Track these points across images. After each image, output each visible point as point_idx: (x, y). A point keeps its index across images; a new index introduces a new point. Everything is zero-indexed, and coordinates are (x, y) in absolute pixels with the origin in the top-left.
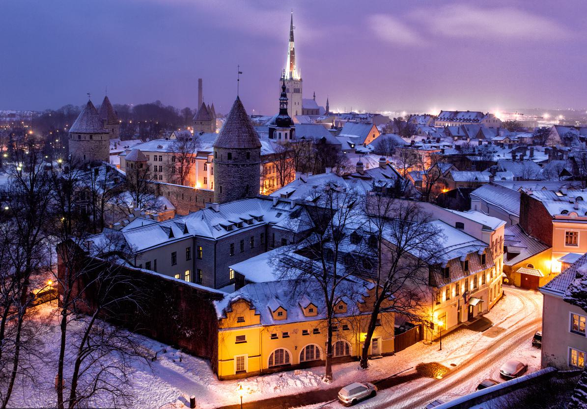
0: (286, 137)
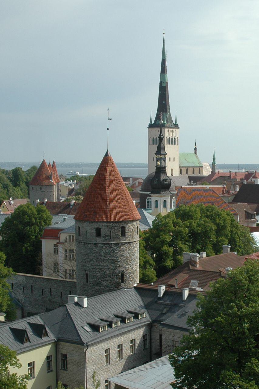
0: (165, 206)
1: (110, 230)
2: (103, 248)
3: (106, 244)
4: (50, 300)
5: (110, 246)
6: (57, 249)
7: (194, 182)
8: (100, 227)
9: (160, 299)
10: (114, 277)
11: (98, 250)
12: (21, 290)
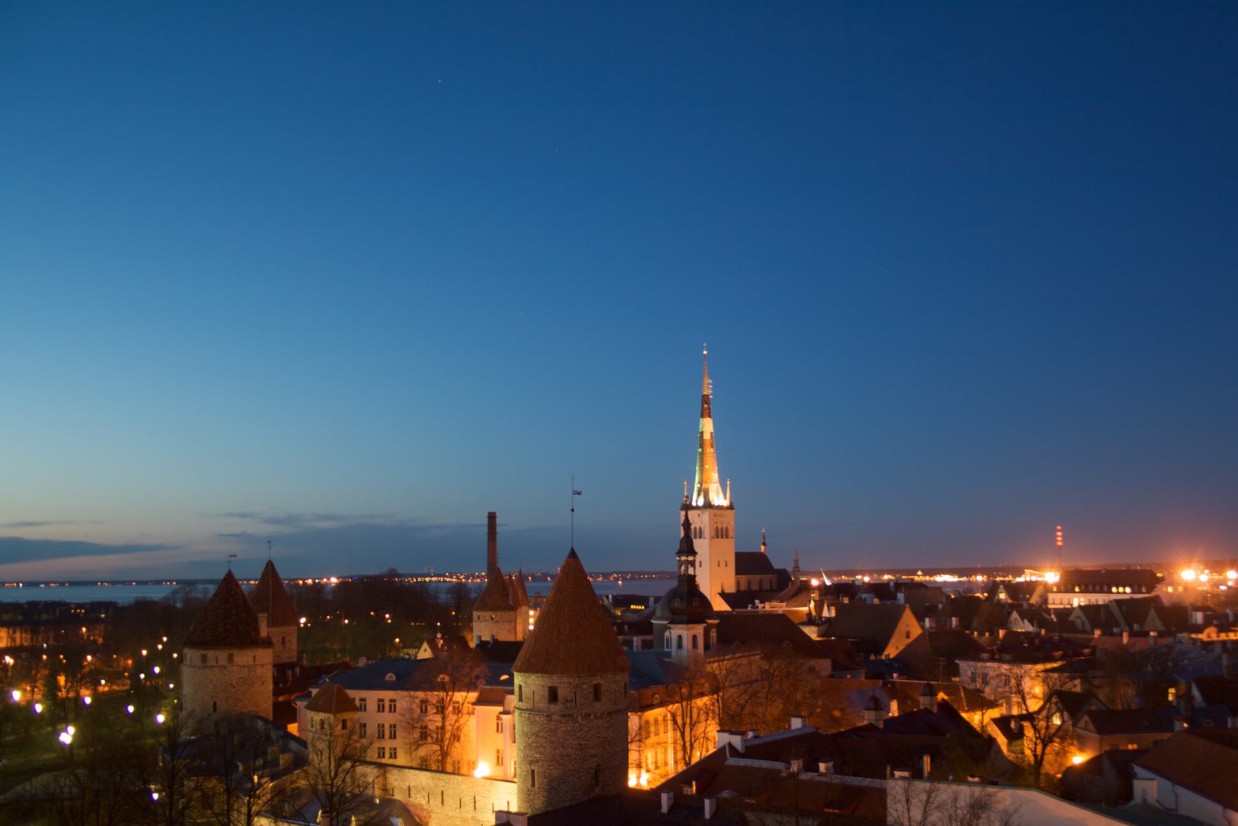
0: (695, 646)
1: (574, 690)
2: (561, 723)
3: (568, 716)
4: (473, 818)
5: (574, 719)
6: (502, 724)
8: (556, 685)
9: (664, 814)
10: (582, 776)
11: (553, 728)
12: (424, 798)
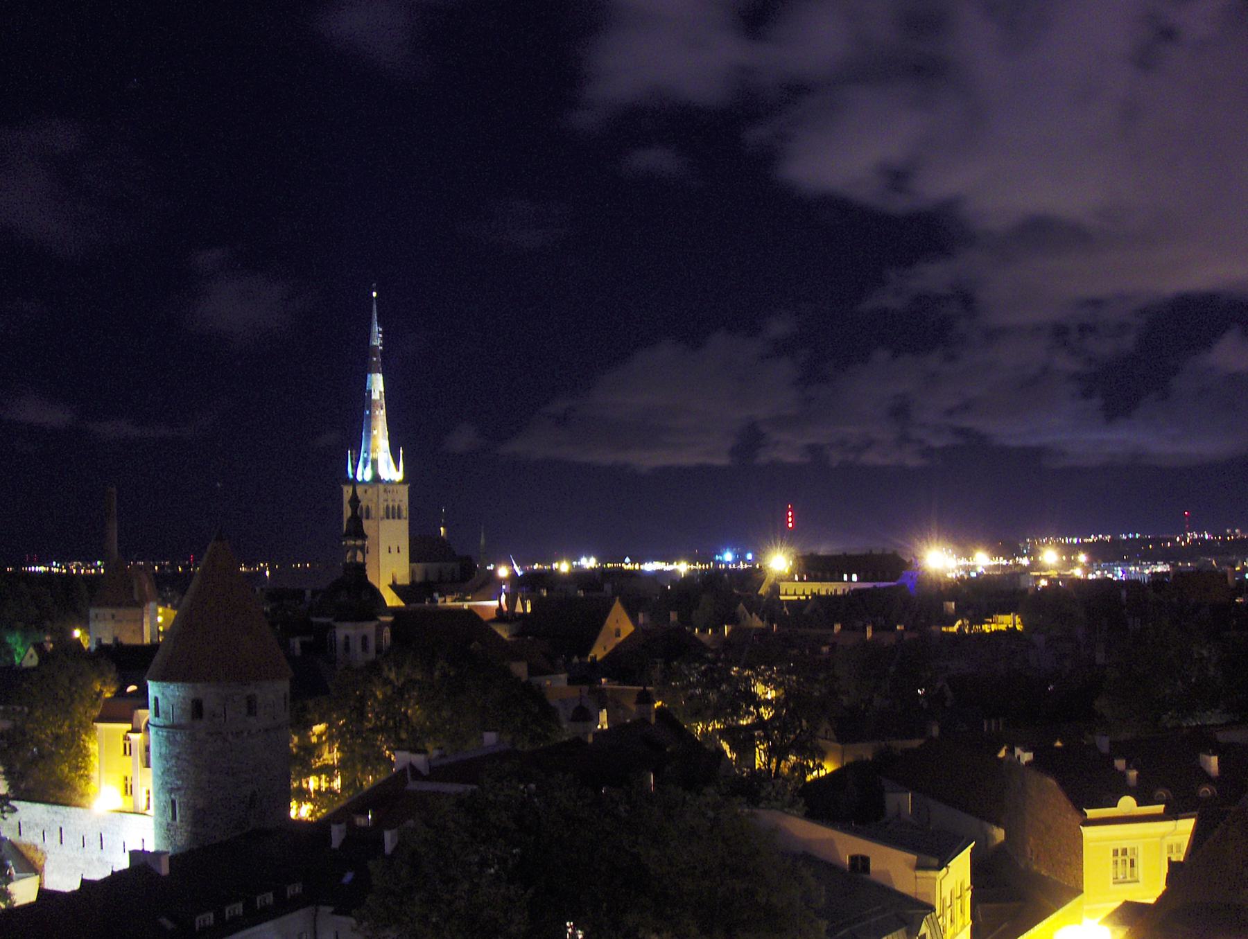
4: (99, 860)
7: (440, 596)
9: (335, 850)
12: (38, 837)
